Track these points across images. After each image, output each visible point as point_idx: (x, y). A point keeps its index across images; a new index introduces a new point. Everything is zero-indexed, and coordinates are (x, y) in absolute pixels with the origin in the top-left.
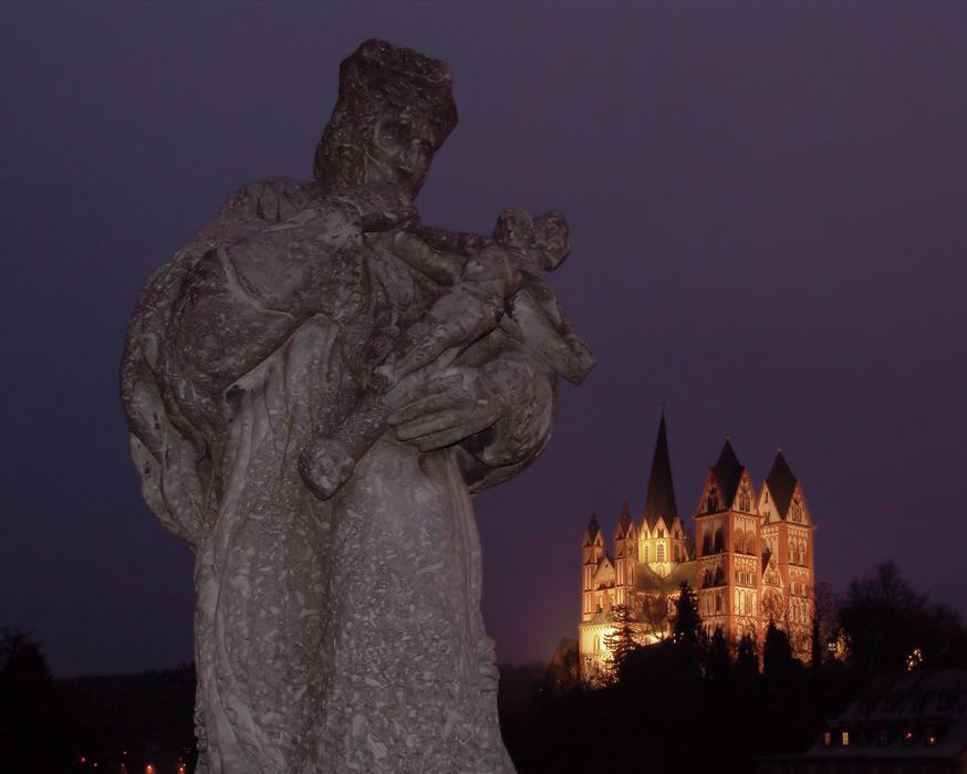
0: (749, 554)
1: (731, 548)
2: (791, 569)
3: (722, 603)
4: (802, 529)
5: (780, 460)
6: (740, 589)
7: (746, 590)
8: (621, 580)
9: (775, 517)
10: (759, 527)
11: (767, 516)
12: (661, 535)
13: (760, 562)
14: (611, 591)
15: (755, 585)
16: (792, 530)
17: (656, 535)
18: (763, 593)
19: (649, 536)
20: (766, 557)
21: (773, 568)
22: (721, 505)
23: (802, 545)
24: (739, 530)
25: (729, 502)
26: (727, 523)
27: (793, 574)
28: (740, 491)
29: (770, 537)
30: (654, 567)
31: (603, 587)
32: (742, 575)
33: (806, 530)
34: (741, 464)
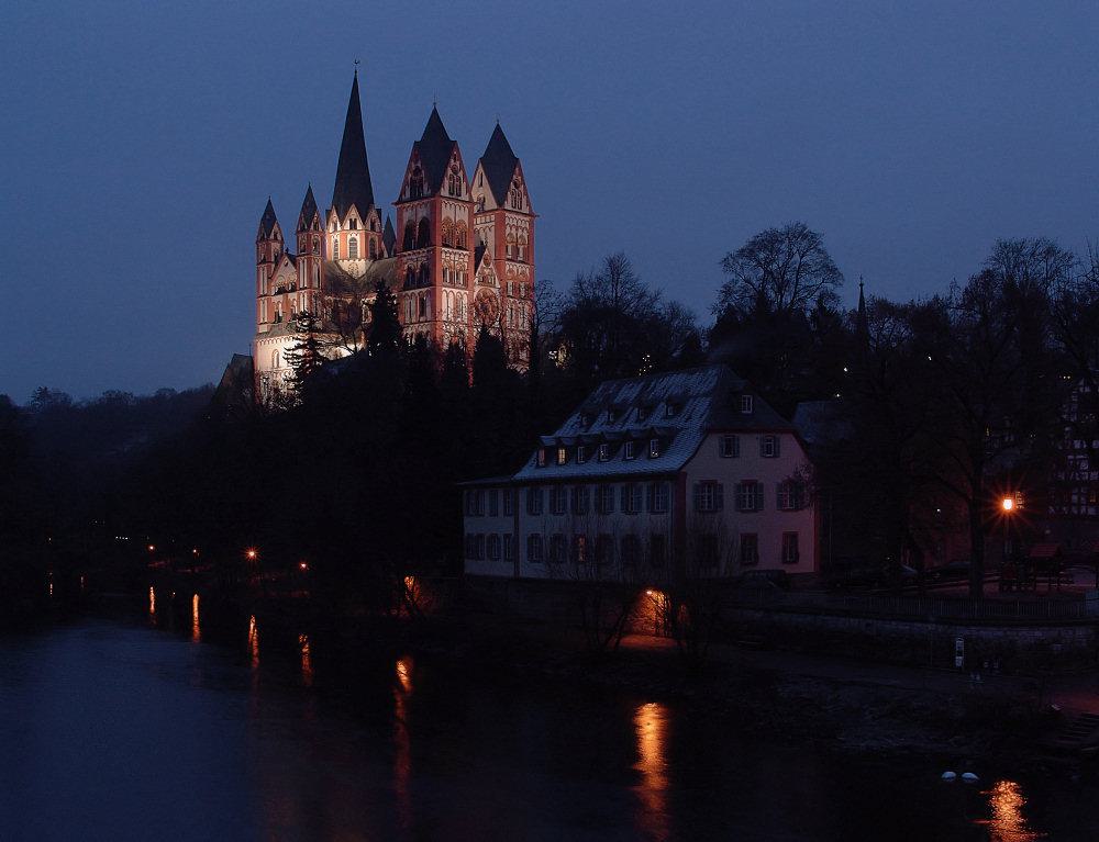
1: (439, 240)
2: (508, 266)
3: (428, 306)
6: (448, 290)
7: (455, 291)
8: (304, 282)
9: (491, 204)
10: (472, 216)
11: (482, 202)
12: (353, 226)
14: (293, 296)
15: (466, 285)
16: (511, 219)
17: (347, 226)
18: (475, 294)
19: (339, 228)
20: (479, 252)
21: (487, 264)
22: (426, 190)
23: (522, 237)
25: (436, 187)
26: (435, 210)
27: (511, 271)
28: (450, 172)
29: (485, 229)
30: (345, 265)
31: (282, 291)
32: (451, 273)
33: (527, 219)
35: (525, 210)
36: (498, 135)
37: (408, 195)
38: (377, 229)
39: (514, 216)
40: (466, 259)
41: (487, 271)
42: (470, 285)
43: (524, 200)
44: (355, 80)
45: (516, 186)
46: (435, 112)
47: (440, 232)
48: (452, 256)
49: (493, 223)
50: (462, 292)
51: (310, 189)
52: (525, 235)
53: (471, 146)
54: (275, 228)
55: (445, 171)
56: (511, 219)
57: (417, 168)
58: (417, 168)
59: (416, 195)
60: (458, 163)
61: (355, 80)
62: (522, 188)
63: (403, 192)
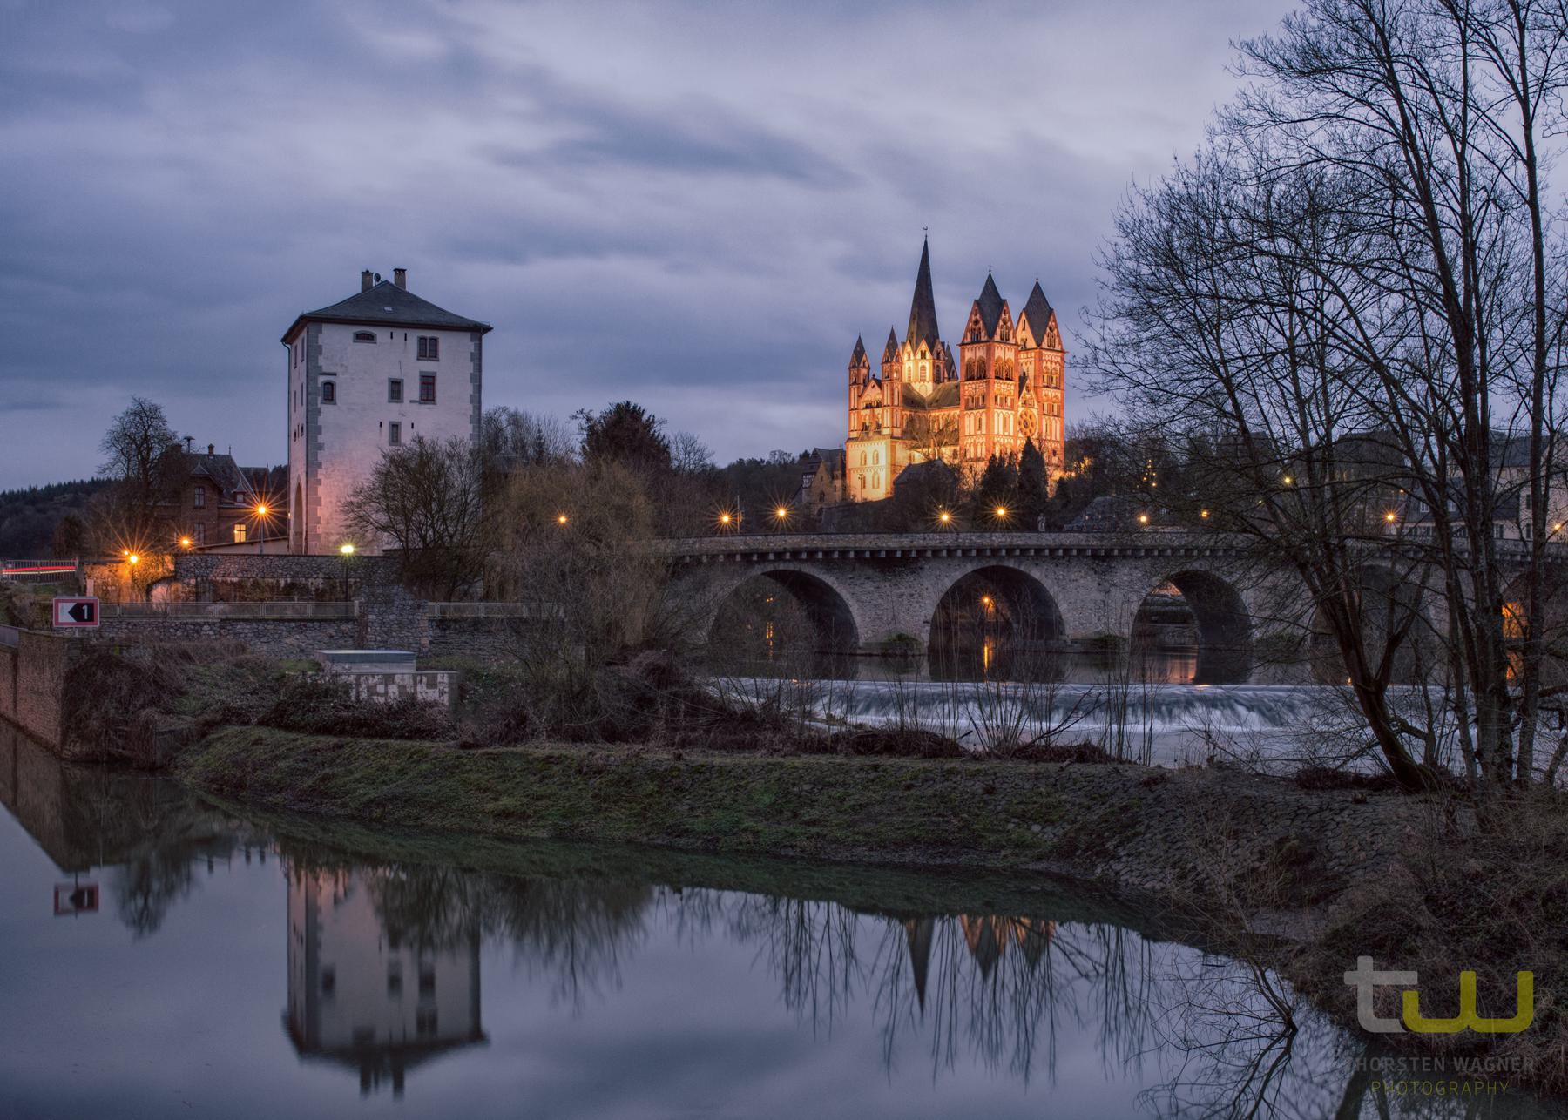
2: (1044, 391)
5: (1037, 292)
8: (887, 401)
9: (1032, 344)
10: (1017, 353)
11: (1025, 341)
12: (923, 355)
14: (877, 411)
15: (1012, 408)
16: (1047, 355)
20: (1023, 379)
22: (984, 337)
26: (990, 352)
29: (1027, 364)
30: (916, 386)
31: (867, 407)
59: (976, 340)
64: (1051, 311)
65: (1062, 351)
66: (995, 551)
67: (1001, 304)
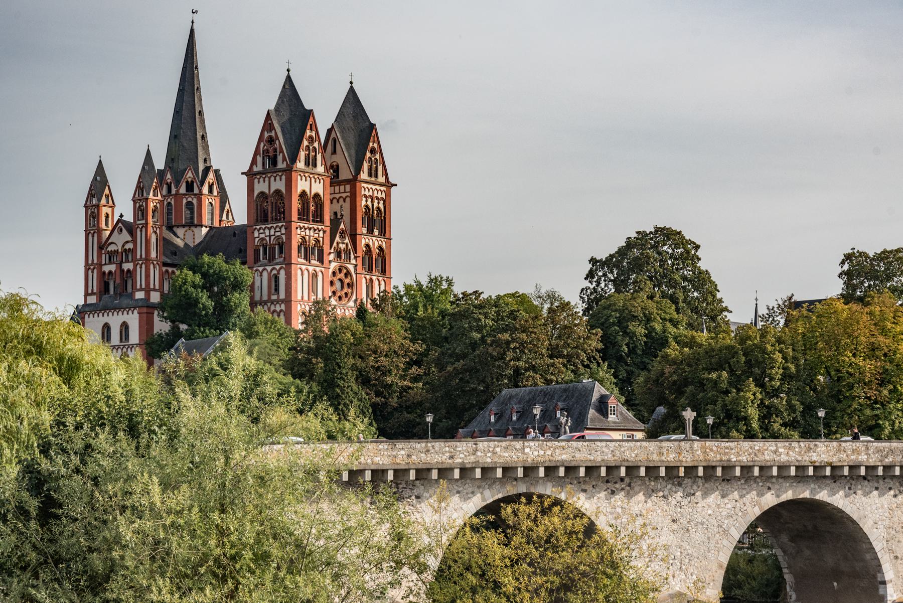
0: (314, 221)
1: (295, 216)
4: (378, 188)
6: (304, 267)
7: (311, 269)
13: (328, 230)
17: (183, 190)
18: (331, 271)
19: (174, 191)
21: (342, 237)
23: (379, 208)
24: (303, 194)
25: (294, 158)
27: (367, 246)
28: (305, 143)
32: (306, 249)
33: (384, 188)
34: (308, 107)
35: (381, 179)
36: (352, 98)
37: (258, 168)
38: (215, 193)
39: (370, 186)
40: (321, 233)
41: (342, 246)
42: (326, 261)
43: (380, 168)
44: (192, 31)
45: (373, 151)
46: (289, 78)
47: (296, 205)
48: (307, 231)
49: (348, 194)
50: (318, 269)
51: (148, 153)
52: (381, 206)
53: (325, 117)
54: (107, 191)
55: (300, 142)
56: (366, 190)
57: (270, 137)
58: (270, 137)
60: (313, 134)
61: (192, 31)
62: (378, 156)
63: (254, 162)
64: (372, 126)
65: (389, 185)
66: (529, 470)
67: (304, 117)
